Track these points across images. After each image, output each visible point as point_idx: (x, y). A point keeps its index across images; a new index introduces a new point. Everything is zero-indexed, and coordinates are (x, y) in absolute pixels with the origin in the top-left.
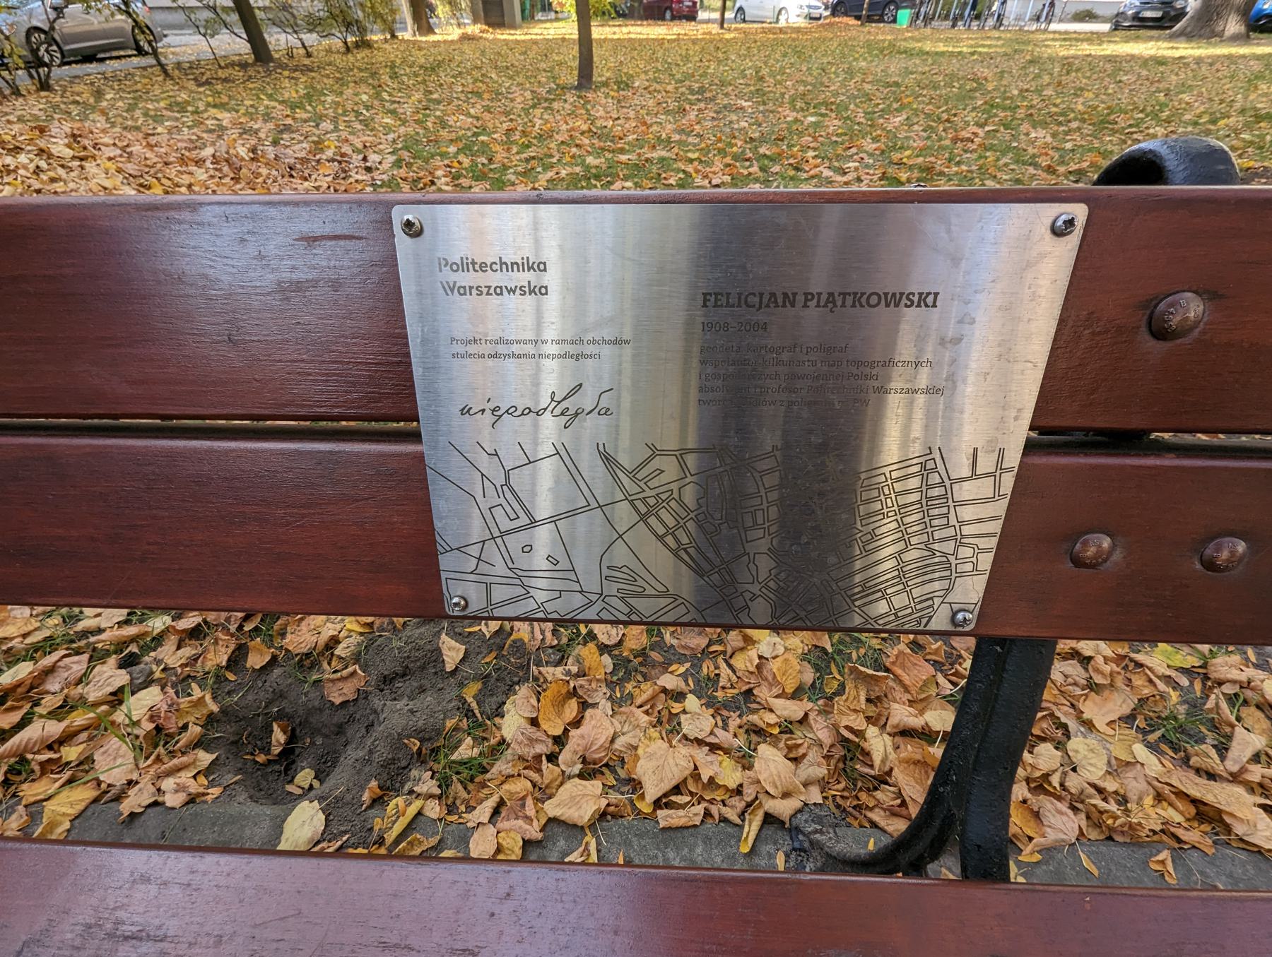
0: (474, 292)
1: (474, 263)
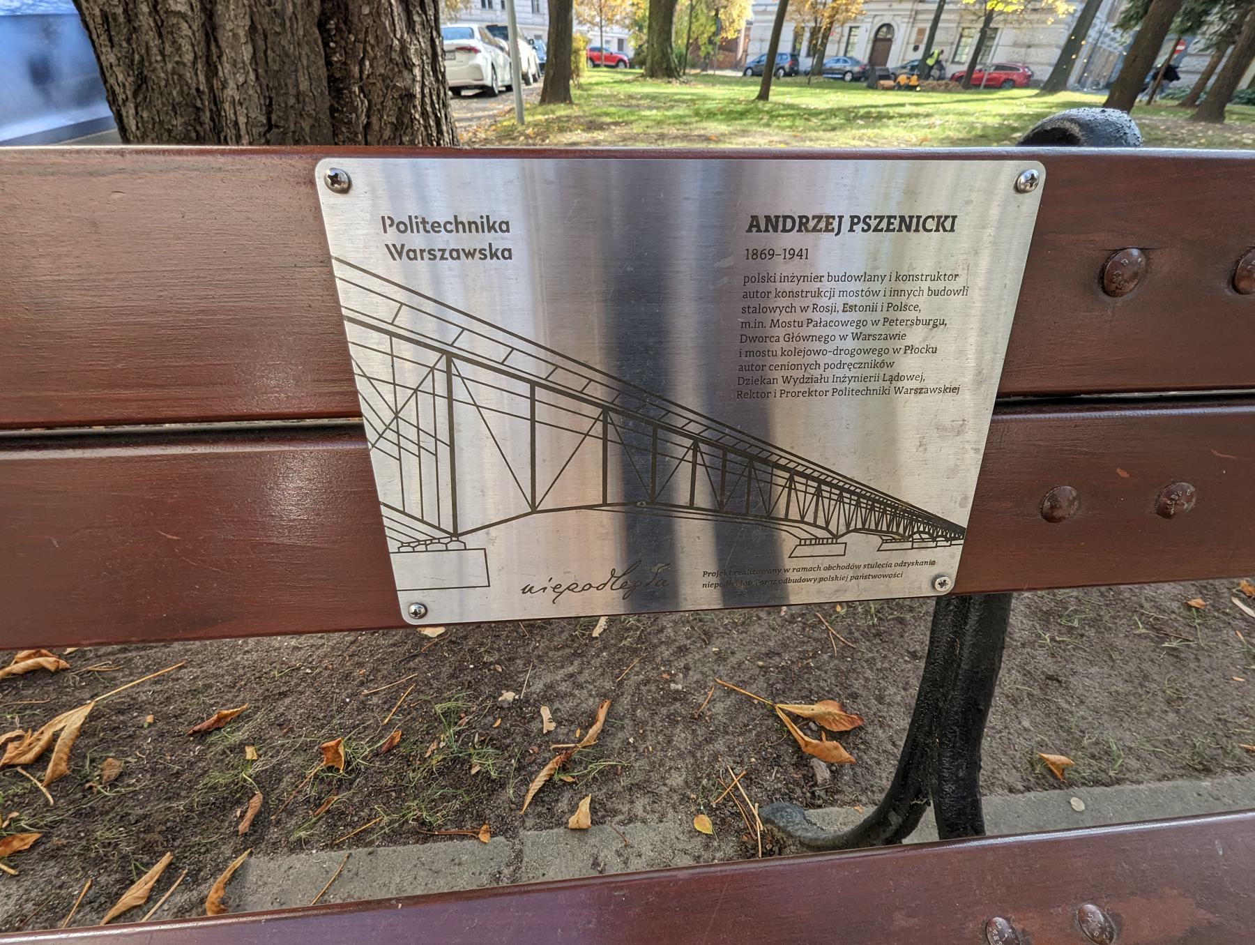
0: (426, 255)
1: (424, 222)
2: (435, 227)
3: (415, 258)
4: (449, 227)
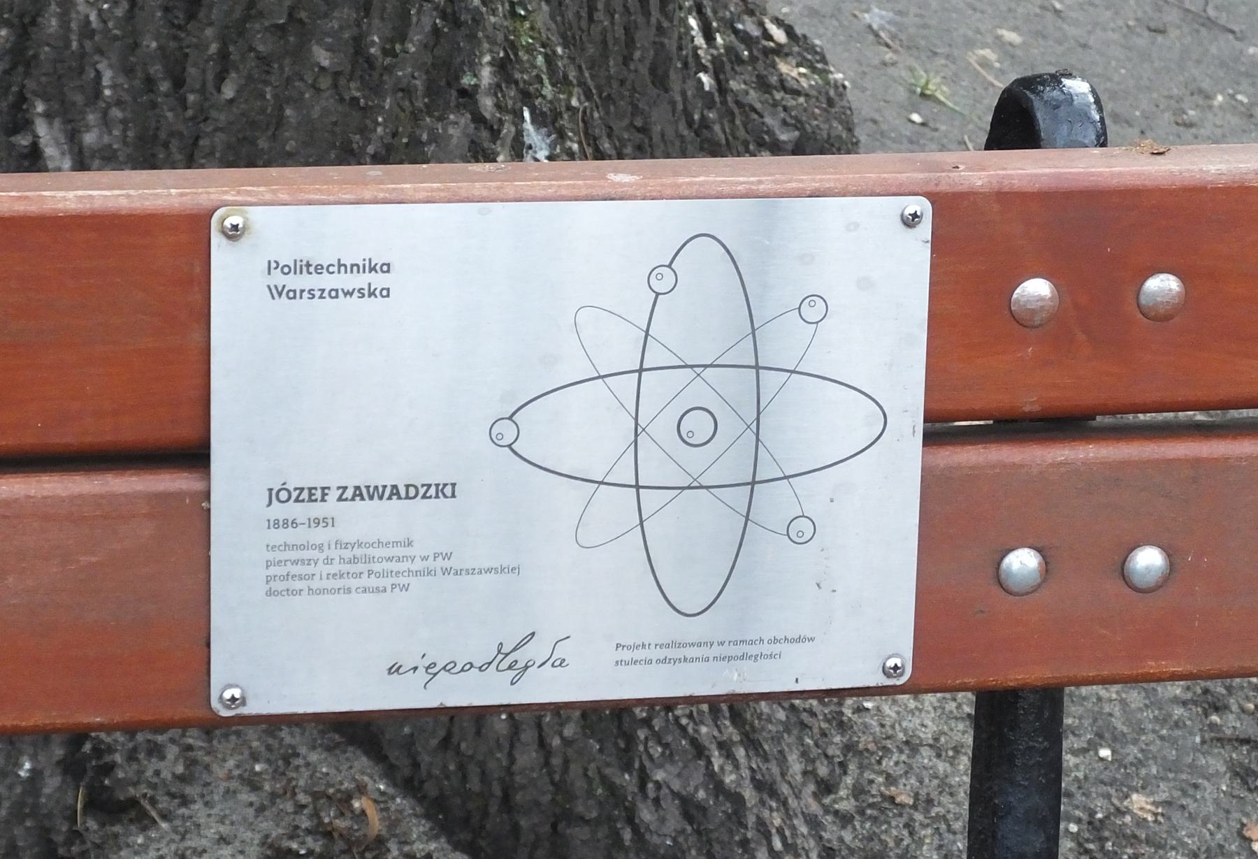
1: (308, 265)
2: (319, 269)
3: (294, 297)
4: (331, 269)
